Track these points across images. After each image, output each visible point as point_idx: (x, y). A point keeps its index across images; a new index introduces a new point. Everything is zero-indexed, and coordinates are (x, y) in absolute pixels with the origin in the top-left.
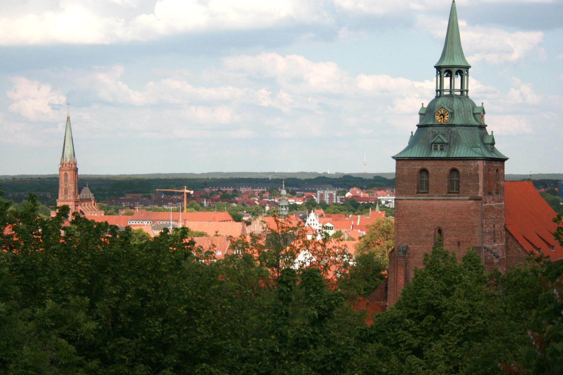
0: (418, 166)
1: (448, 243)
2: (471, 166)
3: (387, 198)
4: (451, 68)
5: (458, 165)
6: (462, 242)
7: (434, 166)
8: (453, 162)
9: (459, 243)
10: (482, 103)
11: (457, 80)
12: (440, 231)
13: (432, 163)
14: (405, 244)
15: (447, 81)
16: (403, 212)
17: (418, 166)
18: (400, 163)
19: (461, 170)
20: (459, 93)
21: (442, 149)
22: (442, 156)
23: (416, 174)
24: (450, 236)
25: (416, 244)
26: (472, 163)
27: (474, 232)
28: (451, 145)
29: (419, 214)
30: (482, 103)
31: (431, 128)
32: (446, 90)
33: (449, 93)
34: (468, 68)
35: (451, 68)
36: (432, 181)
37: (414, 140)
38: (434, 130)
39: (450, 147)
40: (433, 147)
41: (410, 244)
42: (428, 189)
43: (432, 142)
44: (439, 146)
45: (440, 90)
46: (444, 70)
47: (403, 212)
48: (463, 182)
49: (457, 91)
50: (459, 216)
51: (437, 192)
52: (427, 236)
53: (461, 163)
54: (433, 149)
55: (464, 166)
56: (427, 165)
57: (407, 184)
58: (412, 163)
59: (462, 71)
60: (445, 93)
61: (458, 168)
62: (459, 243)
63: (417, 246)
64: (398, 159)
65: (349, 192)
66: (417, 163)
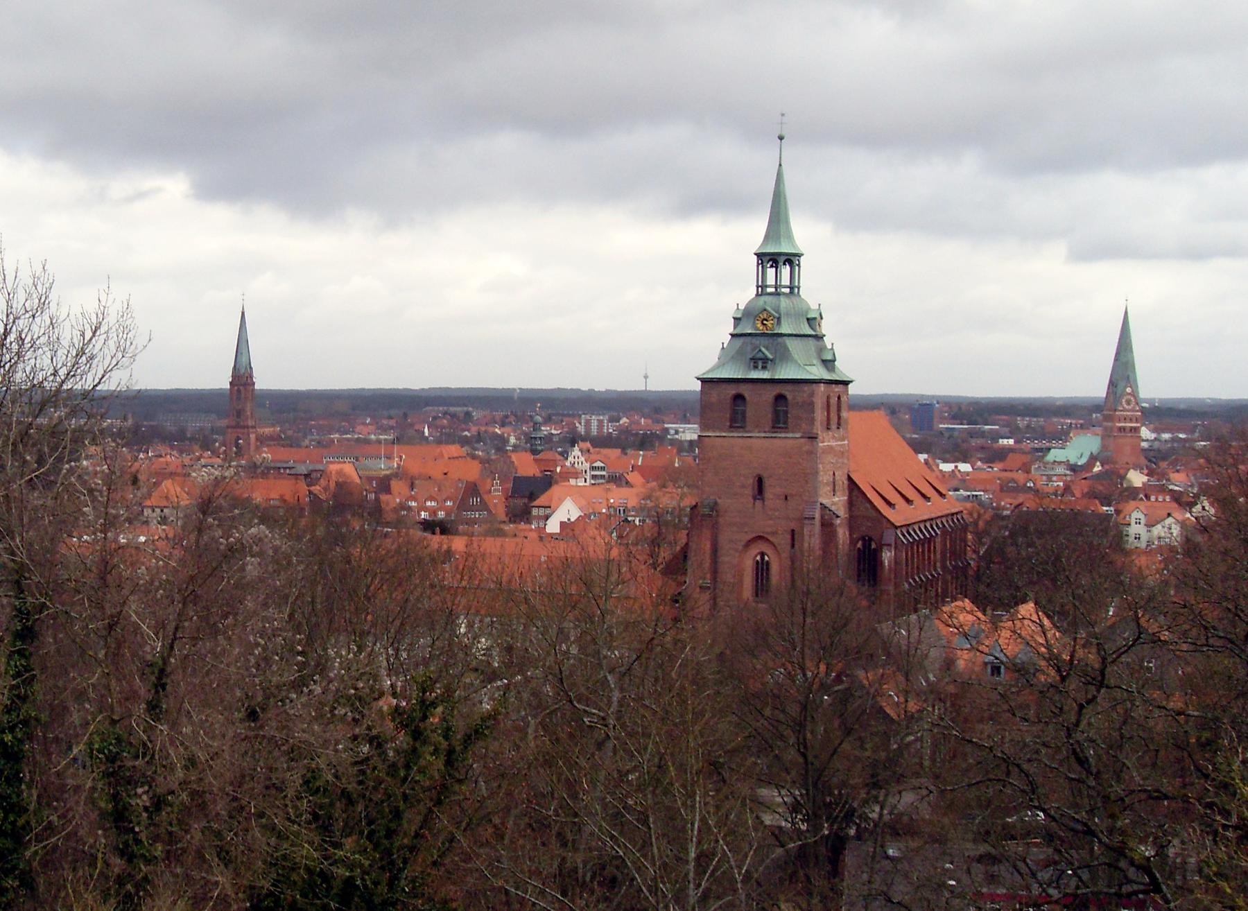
0: (732, 390)
3: (689, 432)
6: (792, 495)
11: (786, 271)
12: (760, 481)
13: (750, 386)
15: (771, 272)
19: (789, 397)
20: (788, 290)
21: (764, 368)
26: (806, 388)
27: (807, 482)
32: (770, 286)
33: (773, 290)
34: (799, 255)
36: (750, 411)
37: (727, 356)
42: (786, 422)
45: (762, 287)
46: (768, 259)
48: (793, 412)
49: (785, 287)
52: (743, 486)
53: (790, 387)
56: (744, 390)
58: (724, 386)
59: (791, 260)
60: (769, 290)
64: (704, 381)
65: (630, 423)
66: (733, 385)
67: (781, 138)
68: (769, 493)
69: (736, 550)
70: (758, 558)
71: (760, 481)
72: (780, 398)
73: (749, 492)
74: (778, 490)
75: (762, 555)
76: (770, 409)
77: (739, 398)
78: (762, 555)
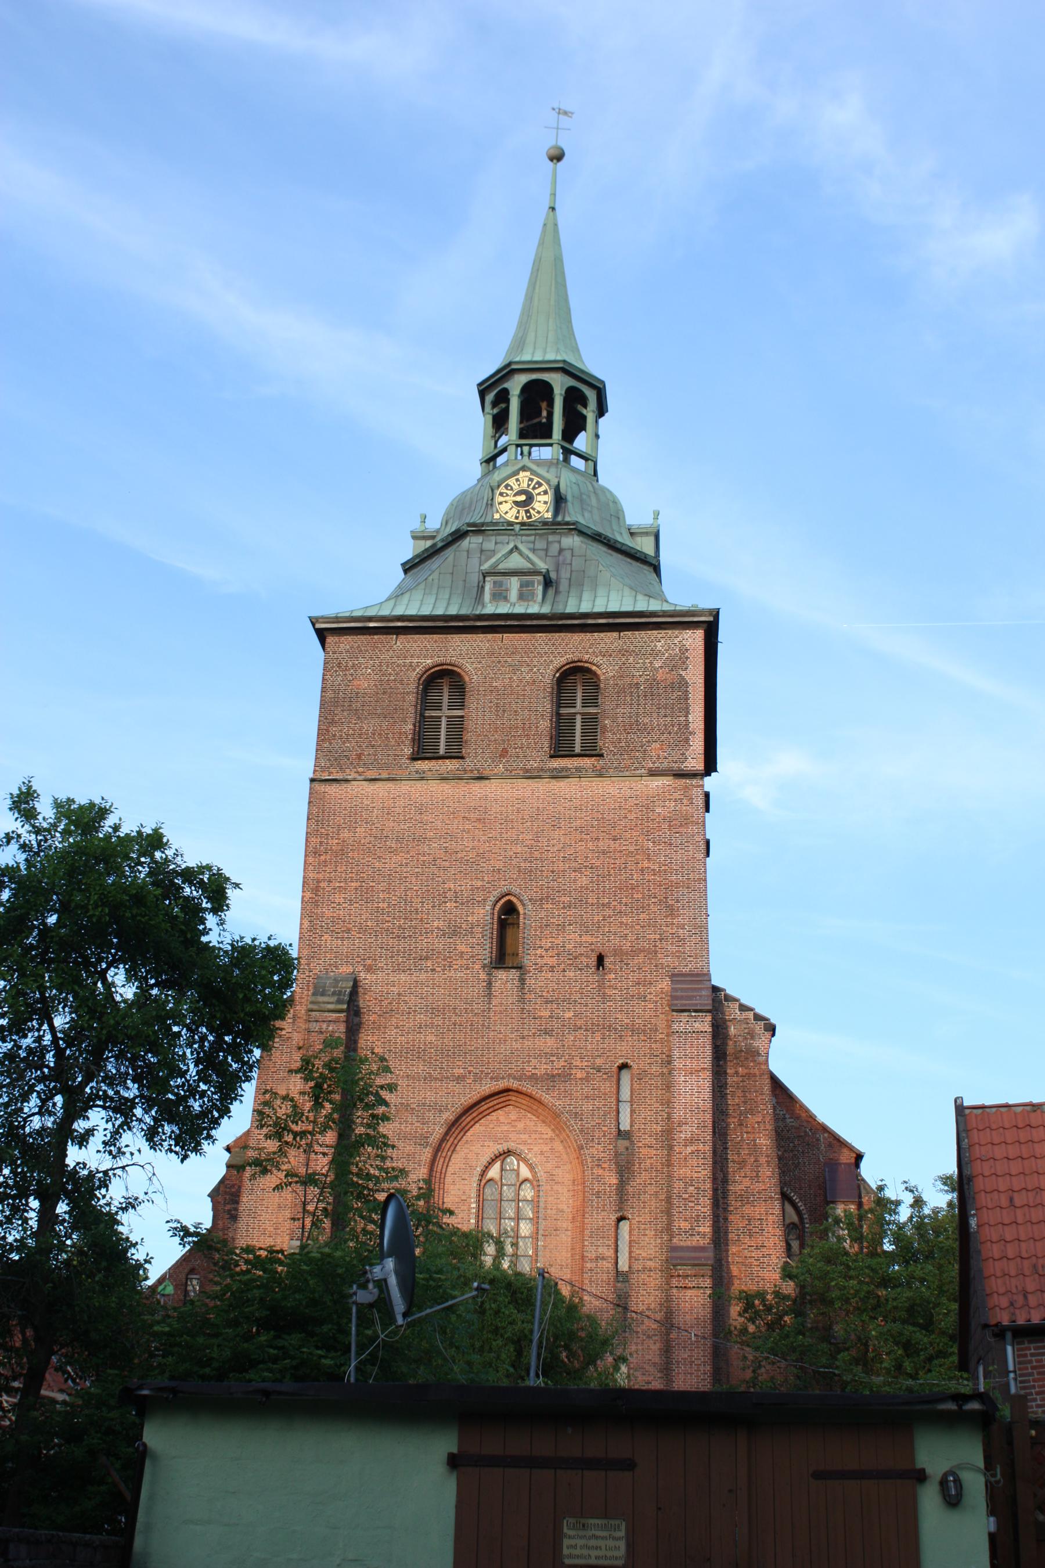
0: (425, 653)
2: (655, 654)
4: (543, 404)
5: (597, 650)
6: (618, 952)
8: (577, 637)
9: (600, 960)
10: (657, 515)
12: (508, 914)
14: (345, 969)
16: (345, 834)
17: (425, 653)
18: (346, 642)
19: (606, 670)
22: (530, 611)
23: (412, 687)
24: (561, 928)
25: (399, 969)
26: (660, 641)
27: (672, 912)
28: (564, 586)
30: (657, 515)
35: (543, 404)
36: (478, 714)
39: (557, 592)
40: (488, 587)
41: (369, 969)
43: (486, 566)
47: (345, 834)
51: (504, 753)
52: (454, 932)
53: (609, 639)
55: (624, 652)
56: (462, 652)
57: (369, 726)
61: (598, 660)
62: (600, 960)
63: (403, 977)
67: (557, 157)
68: (536, 944)
71: (508, 914)
74: (572, 938)
76: (546, 706)
77: (442, 680)
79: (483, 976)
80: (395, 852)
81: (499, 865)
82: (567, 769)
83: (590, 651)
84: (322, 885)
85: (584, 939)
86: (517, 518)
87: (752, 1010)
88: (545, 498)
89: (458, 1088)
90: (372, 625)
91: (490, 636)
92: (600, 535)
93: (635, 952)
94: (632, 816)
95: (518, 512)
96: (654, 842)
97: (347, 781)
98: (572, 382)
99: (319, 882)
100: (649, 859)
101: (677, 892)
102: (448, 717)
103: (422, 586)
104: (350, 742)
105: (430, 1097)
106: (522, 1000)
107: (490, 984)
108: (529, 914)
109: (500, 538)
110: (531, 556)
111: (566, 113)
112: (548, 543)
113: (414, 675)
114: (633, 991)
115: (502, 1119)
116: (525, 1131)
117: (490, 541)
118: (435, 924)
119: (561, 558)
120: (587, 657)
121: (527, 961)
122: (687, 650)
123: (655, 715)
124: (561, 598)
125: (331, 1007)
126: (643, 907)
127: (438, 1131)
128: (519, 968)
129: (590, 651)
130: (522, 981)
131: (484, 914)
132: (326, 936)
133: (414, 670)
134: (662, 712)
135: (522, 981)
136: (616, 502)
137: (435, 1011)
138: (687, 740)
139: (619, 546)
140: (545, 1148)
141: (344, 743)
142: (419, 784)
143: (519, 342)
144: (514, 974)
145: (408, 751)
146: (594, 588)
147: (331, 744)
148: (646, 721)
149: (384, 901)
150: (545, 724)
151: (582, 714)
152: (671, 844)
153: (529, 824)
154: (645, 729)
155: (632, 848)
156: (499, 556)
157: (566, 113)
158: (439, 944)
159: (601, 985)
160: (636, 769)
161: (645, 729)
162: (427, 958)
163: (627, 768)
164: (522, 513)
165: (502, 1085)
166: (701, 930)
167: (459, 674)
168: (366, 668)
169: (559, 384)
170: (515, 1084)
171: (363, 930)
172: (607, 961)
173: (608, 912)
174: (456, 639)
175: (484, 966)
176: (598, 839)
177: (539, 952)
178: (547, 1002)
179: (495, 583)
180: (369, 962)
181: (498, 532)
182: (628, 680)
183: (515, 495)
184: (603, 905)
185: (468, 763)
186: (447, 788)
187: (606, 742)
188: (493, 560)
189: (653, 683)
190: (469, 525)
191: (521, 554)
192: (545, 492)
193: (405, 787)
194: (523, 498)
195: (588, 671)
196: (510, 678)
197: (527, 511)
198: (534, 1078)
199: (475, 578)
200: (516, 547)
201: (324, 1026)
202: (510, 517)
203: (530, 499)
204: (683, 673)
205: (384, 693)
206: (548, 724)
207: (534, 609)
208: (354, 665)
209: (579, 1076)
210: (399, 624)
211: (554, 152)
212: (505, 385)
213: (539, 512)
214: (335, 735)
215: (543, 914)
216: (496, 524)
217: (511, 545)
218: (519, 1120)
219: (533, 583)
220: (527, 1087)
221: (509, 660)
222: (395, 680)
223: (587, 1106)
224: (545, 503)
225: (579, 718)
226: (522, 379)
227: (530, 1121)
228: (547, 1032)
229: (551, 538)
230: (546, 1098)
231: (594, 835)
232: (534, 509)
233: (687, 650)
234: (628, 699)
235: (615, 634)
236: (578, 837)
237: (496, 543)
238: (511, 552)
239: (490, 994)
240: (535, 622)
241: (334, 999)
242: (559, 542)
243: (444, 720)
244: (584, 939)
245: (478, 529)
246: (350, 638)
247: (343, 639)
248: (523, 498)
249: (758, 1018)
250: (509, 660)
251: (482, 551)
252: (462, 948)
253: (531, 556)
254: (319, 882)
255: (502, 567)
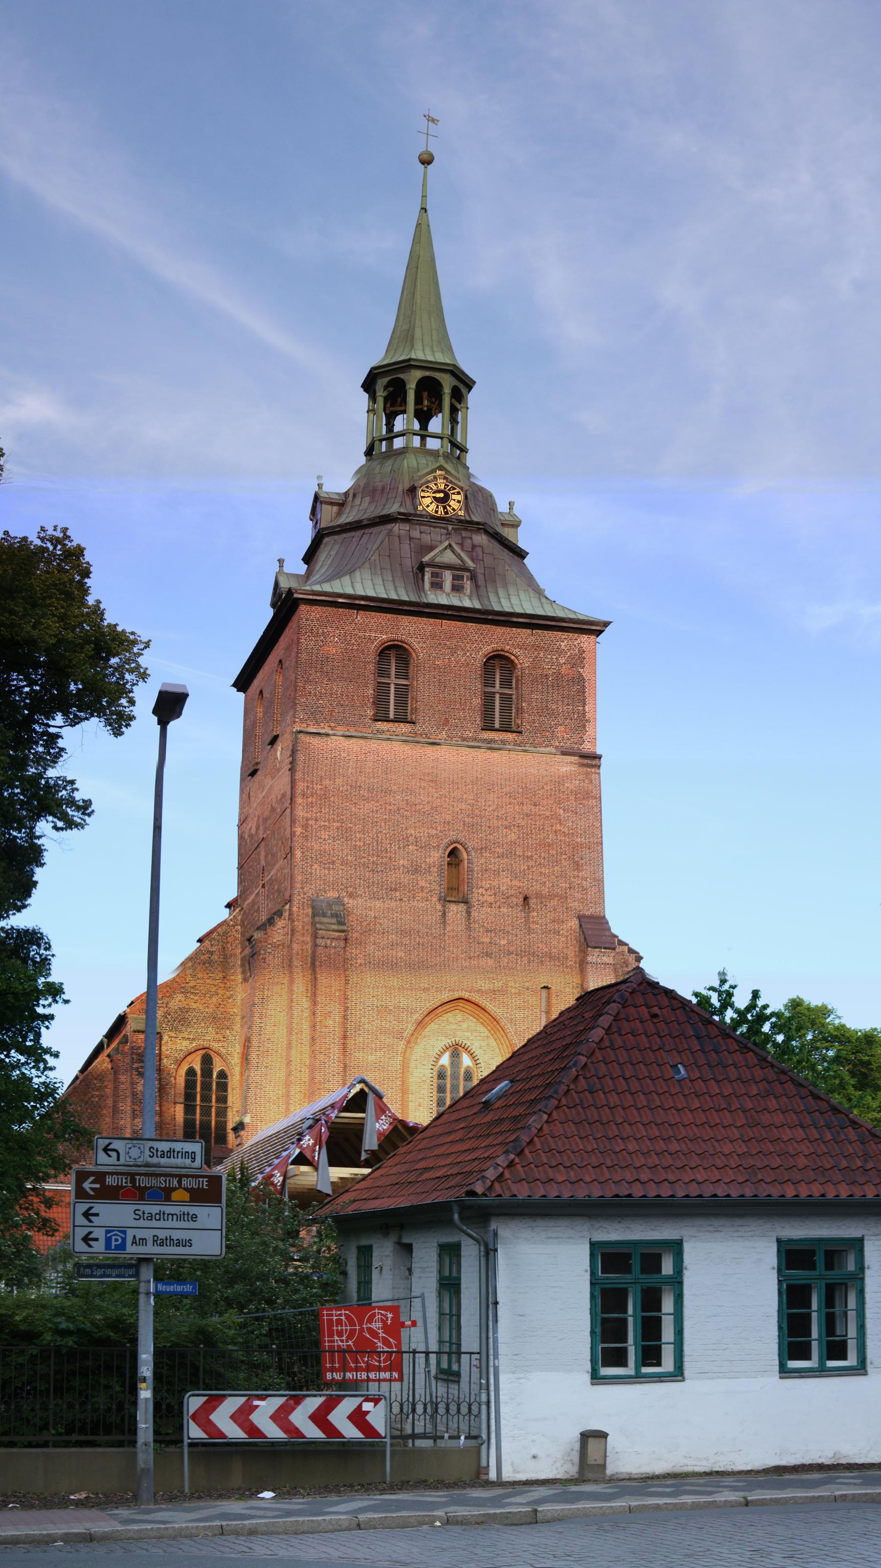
1: (491, 899)
2: (560, 652)
4: (416, 390)
5: (516, 643)
6: (539, 895)
7: (433, 636)
8: (500, 630)
13: (425, 625)
14: (332, 894)
17: (381, 629)
19: (523, 660)
21: (457, 588)
24: (497, 873)
25: (374, 897)
26: (564, 641)
27: (578, 867)
29: (388, 792)
31: (407, 527)
35: (416, 390)
36: (424, 688)
38: (415, 534)
40: (427, 577)
41: (351, 895)
43: (426, 559)
44: (448, 576)
48: (531, 699)
50: (527, 808)
52: (416, 870)
54: (427, 585)
55: (536, 647)
56: (411, 630)
57: (337, 687)
58: (360, 617)
62: (526, 898)
63: (378, 904)
67: (426, 161)
69: (399, 1035)
70: (445, 1060)
72: (498, 663)
73: (432, 882)
74: (505, 882)
75: (456, 1051)
76: (478, 685)
78: (456, 1051)
79: (439, 907)
80: (367, 800)
81: (449, 818)
82: (495, 741)
83: (511, 643)
84: (310, 822)
85: (514, 883)
86: (436, 512)
87: (626, 945)
88: (458, 497)
89: (424, 996)
90: (340, 600)
91: (432, 620)
92: (497, 533)
93: (551, 896)
94: (548, 788)
95: (437, 507)
96: (564, 810)
97: (327, 735)
98: (455, 382)
99: (307, 820)
100: (561, 824)
101: (581, 853)
102: (396, 684)
103: (367, 565)
104: (323, 700)
105: (404, 1002)
106: (469, 928)
107: (444, 914)
108: (475, 861)
109: (424, 528)
110: (462, 554)
111: (433, 120)
112: (463, 538)
113: (373, 647)
114: (550, 926)
115: (451, 1020)
116: (468, 1030)
117: (416, 530)
118: (401, 862)
119: (474, 553)
120: (508, 648)
121: (474, 898)
122: (584, 652)
123: (560, 703)
124: (482, 590)
125: (335, 927)
126: (557, 862)
127: (410, 1027)
128: (466, 902)
129: (511, 643)
130: (469, 913)
131: (437, 857)
132: (316, 866)
133: (373, 643)
134: (566, 701)
135: (469, 913)
136: (491, 496)
137: (404, 933)
138: (584, 726)
139: (507, 542)
140: (484, 1044)
141: (318, 700)
142: (385, 743)
143: (403, 334)
144: (462, 907)
145: (370, 712)
146: (505, 586)
147: (307, 699)
148: (554, 707)
149: (360, 840)
150: (477, 701)
151: (501, 694)
152: (576, 813)
153: (470, 786)
154: (553, 714)
155: (548, 814)
156: (437, 551)
157: (433, 120)
158: (405, 879)
159: (527, 921)
160: (547, 746)
161: (553, 714)
162: (396, 890)
163: (540, 745)
164: (441, 509)
165: (457, 995)
166: (599, 882)
167: (406, 650)
168: (334, 636)
169: (447, 383)
170: (466, 995)
171: (344, 863)
172: (532, 902)
173: (531, 863)
174: (405, 620)
175: (439, 900)
176: (522, 803)
177: (480, 891)
178: (487, 931)
179: (432, 573)
180: (350, 889)
181: (421, 524)
182: (540, 671)
183: (434, 493)
184: (528, 857)
185: (418, 728)
186: (407, 749)
187: (526, 721)
188: (432, 554)
189: (558, 676)
190: (400, 514)
191: (453, 551)
192: (459, 493)
193: (373, 745)
194: (442, 495)
195: (507, 659)
196: (448, 657)
197: (445, 508)
198: (479, 991)
199: (409, 564)
200: (450, 545)
201: (329, 942)
202: (432, 509)
203: (447, 498)
204: (581, 671)
205: (349, 660)
206: (479, 701)
207: (467, 603)
208: (323, 633)
209: (513, 991)
210: (363, 603)
211: (425, 157)
212: (401, 376)
213: (454, 509)
214: (310, 692)
215: (483, 861)
216: (421, 516)
217: (446, 543)
218: (463, 1021)
219: (463, 577)
220: (475, 998)
221: (448, 643)
222: (357, 650)
223: (519, 1015)
224: (459, 502)
225: (497, 696)
226: (418, 374)
227: (472, 1023)
228: (489, 955)
229: (464, 534)
230: (490, 1007)
231: (520, 800)
232: (450, 506)
233: (584, 652)
234: (540, 687)
235: (529, 631)
236: (508, 800)
237: (421, 532)
238: (446, 548)
239: (445, 922)
240: (470, 615)
241: (334, 920)
242: (471, 538)
243: (392, 687)
244: (514, 883)
245: (406, 518)
246: (319, 608)
247: (313, 608)
248: (442, 495)
249: (631, 951)
250: (448, 643)
251: (410, 538)
252: (423, 883)
253: (462, 554)
254: (307, 820)
255: (437, 560)
